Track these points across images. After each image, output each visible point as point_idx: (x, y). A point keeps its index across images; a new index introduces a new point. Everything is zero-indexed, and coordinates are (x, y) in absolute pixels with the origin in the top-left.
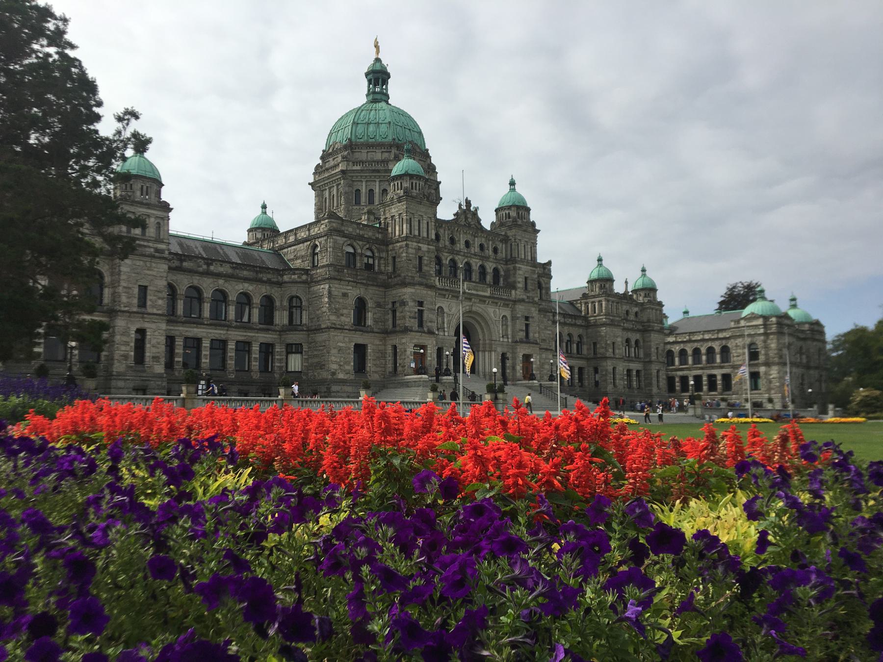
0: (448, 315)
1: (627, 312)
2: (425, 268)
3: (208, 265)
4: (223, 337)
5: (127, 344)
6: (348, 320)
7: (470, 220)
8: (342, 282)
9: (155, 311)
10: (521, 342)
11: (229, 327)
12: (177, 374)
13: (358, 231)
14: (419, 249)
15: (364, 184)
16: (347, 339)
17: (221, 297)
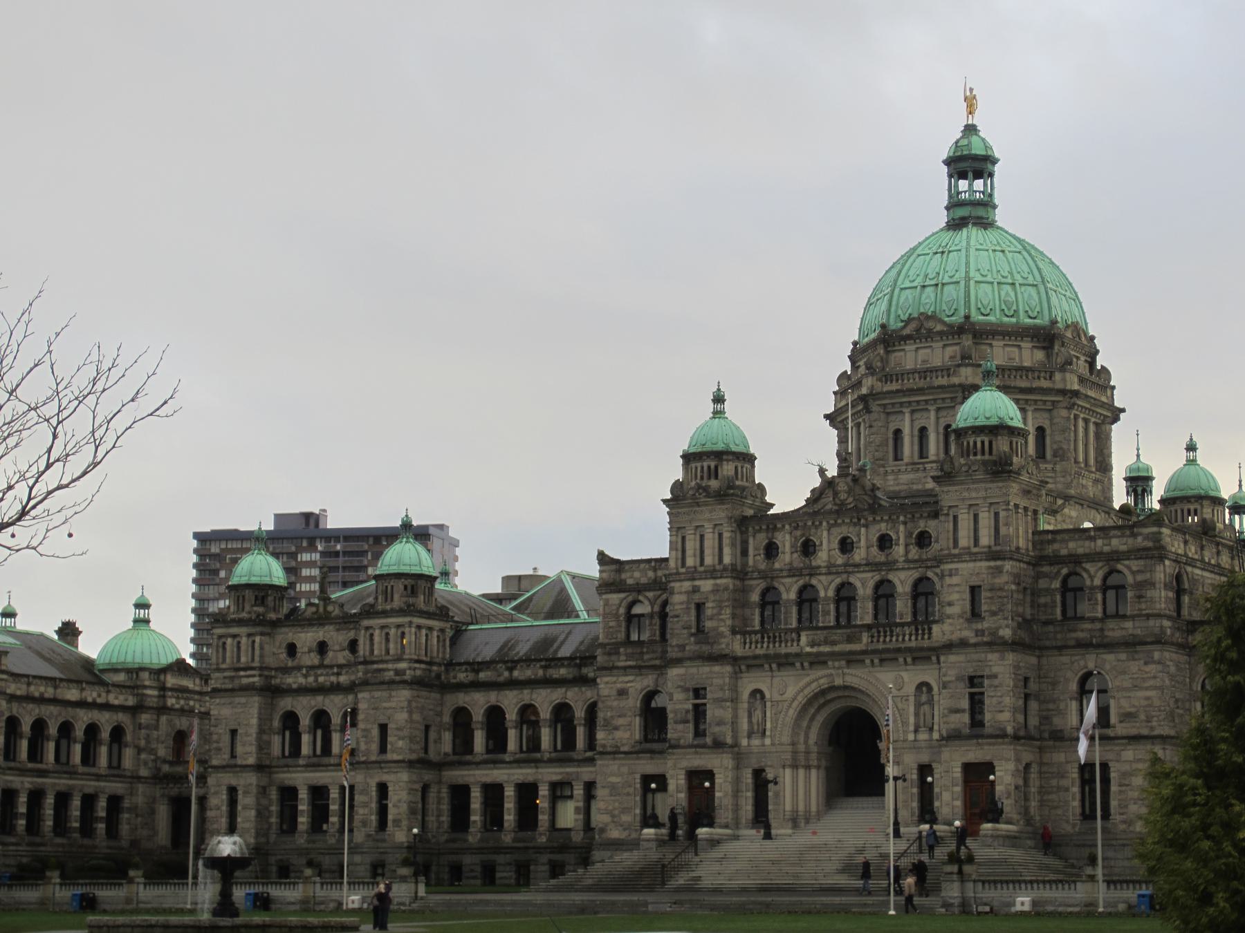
0: (775, 703)
2: (708, 624)
3: (511, 670)
4: (530, 779)
5: (365, 805)
6: (627, 735)
7: (843, 496)
8: (615, 672)
9: (396, 757)
10: (954, 737)
11: (537, 762)
12: (470, 839)
13: (651, 574)
14: (696, 590)
15: (907, 416)
16: (625, 770)
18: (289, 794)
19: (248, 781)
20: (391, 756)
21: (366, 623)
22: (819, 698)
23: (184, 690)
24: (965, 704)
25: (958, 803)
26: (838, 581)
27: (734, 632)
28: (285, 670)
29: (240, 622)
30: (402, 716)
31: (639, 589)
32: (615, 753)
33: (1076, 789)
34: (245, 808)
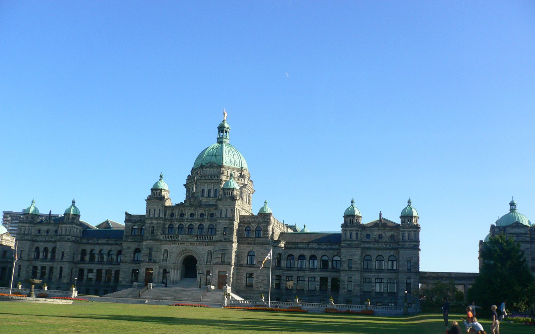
1: (380, 236)
2: (155, 232)
3: (98, 240)
4: (100, 268)
10: (217, 264)
11: (103, 264)
14: (152, 223)
17: (101, 253)
18: (35, 268)
19: (25, 264)
20: (64, 260)
21: (61, 225)
22: (183, 252)
23: (7, 240)
24: (220, 256)
25: (217, 281)
26: (189, 223)
27: (161, 234)
28: (37, 236)
29: (26, 223)
30: (68, 250)
31: (135, 222)
32: (126, 262)
33: (245, 279)
34: (23, 271)
